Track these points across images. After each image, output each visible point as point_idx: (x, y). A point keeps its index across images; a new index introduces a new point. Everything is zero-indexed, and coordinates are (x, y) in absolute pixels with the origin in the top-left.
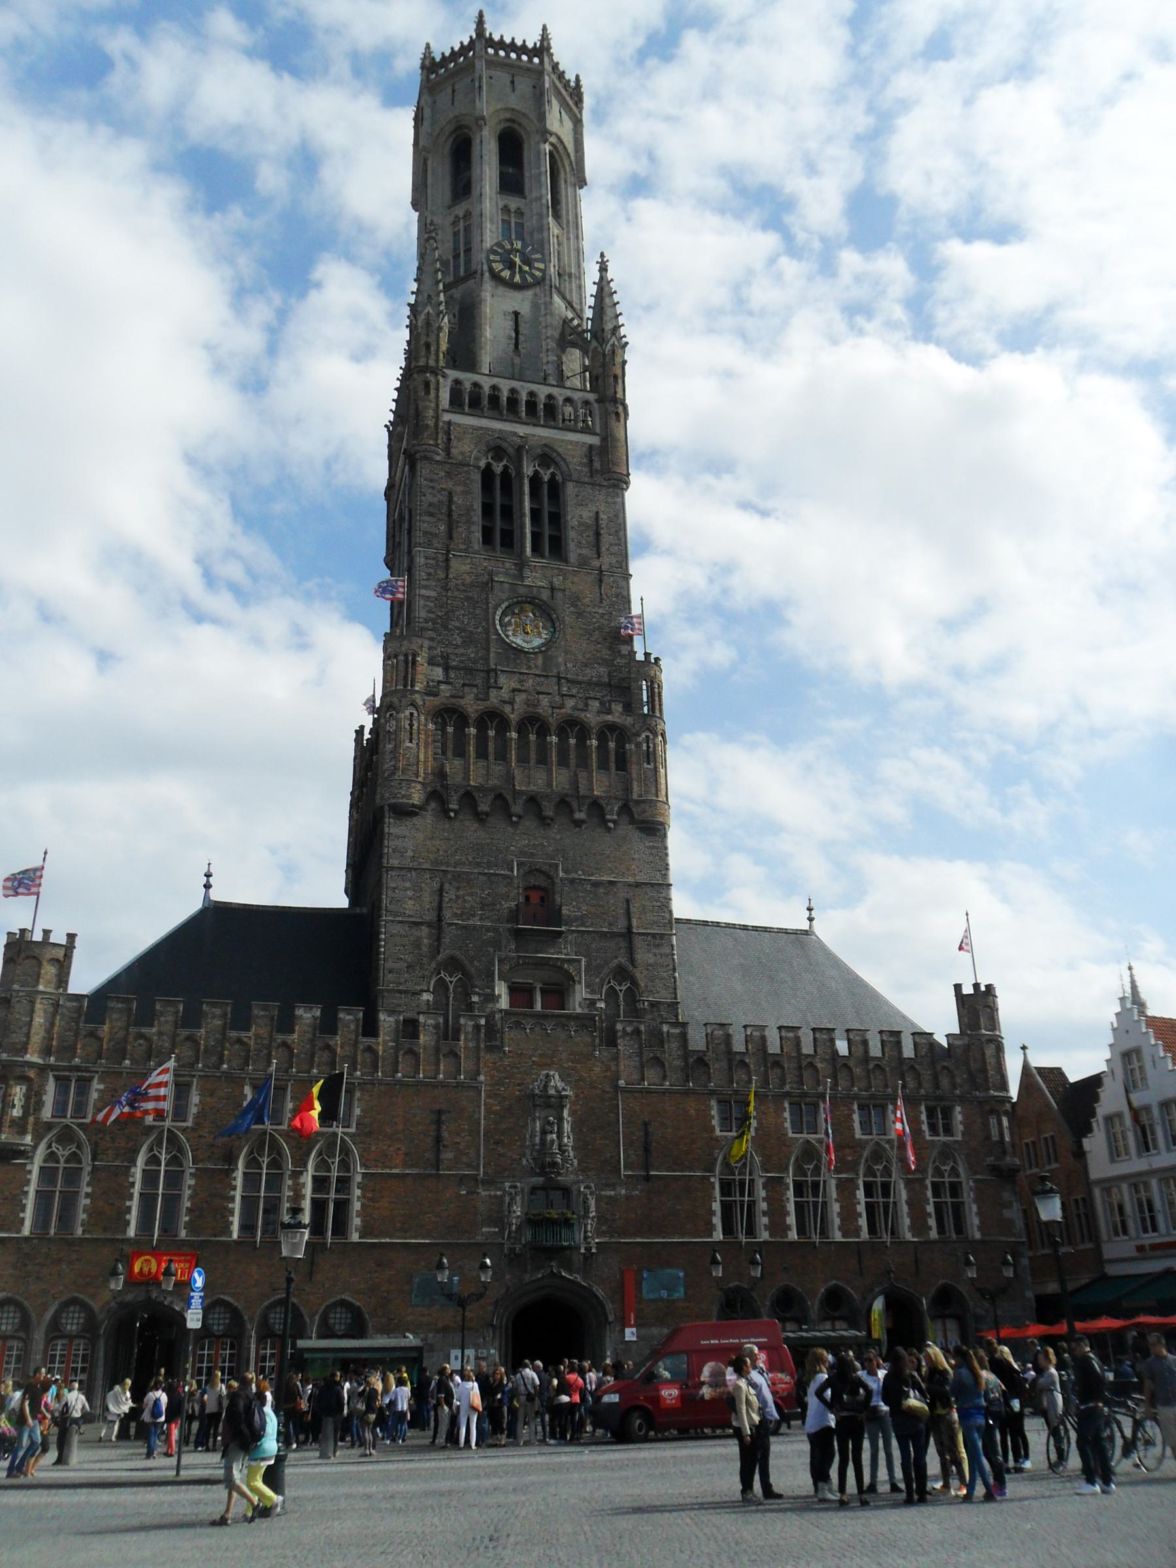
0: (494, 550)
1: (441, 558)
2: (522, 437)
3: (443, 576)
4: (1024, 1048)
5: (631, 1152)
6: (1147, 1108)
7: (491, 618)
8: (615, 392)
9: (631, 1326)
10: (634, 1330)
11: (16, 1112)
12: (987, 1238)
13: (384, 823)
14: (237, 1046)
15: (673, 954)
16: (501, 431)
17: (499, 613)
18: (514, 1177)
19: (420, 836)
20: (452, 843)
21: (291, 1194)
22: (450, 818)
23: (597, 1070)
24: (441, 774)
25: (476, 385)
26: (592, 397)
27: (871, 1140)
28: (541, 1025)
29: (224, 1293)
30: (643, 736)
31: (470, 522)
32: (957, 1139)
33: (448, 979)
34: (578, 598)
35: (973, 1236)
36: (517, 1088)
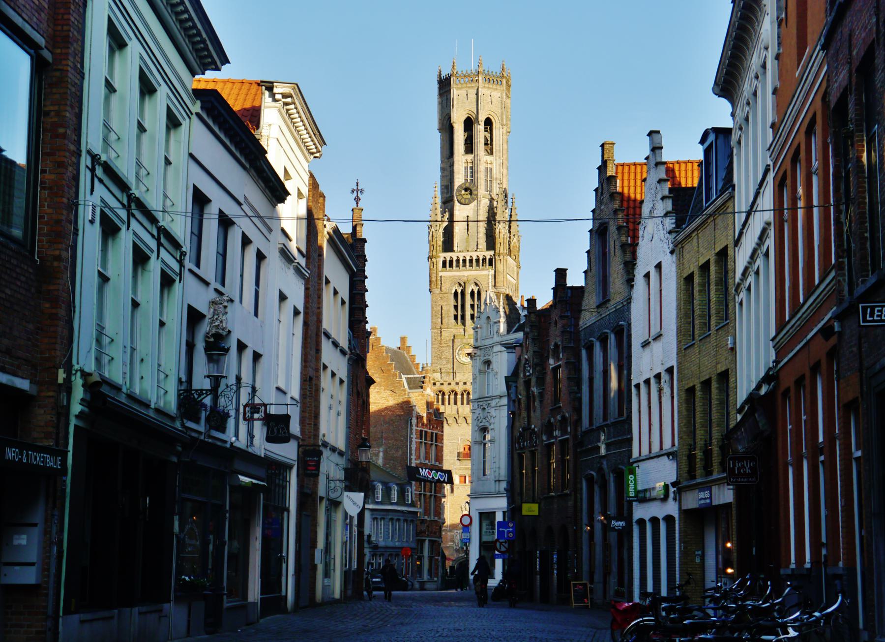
3: (439, 338)
16: (459, 276)
17: (457, 351)
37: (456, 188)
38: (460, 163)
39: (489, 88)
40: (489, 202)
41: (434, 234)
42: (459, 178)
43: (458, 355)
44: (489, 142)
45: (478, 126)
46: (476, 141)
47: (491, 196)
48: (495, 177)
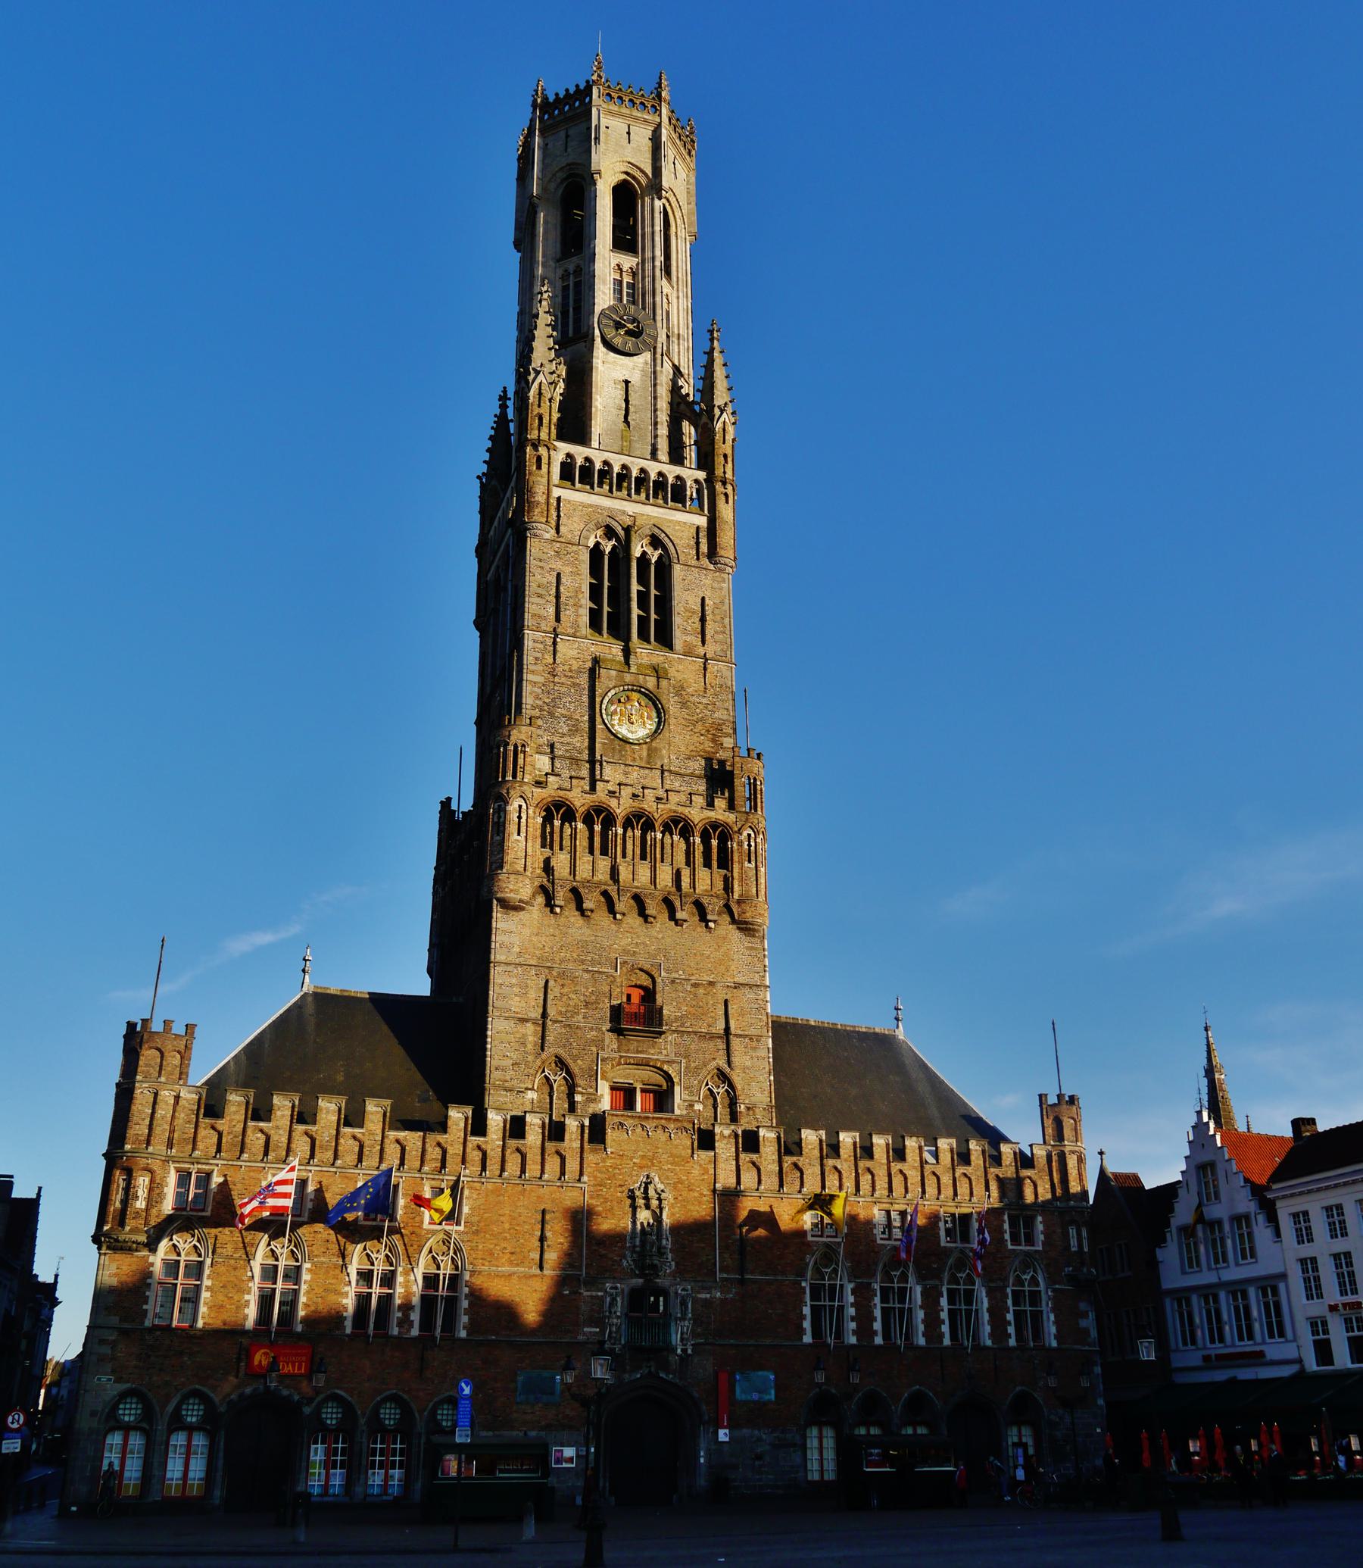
0: (601, 634)
1: (550, 642)
4: (1101, 1153)
5: (726, 1256)
6: (1219, 1222)
7: (598, 706)
8: (725, 473)
9: (725, 1428)
10: (727, 1431)
11: (140, 1204)
12: (1064, 1346)
13: (491, 917)
14: (352, 1141)
15: (769, 1057)
18: (614, 1278)
19: (527, 932)
20: (557, 939)
21: (403, 1291)
22: (557, 914)
23: (696, 1172)
24: (548, 868)
25: (587, 459)
26: (701, 475)
27: (956, 1248)
28: (642, 1126)
29: (338, 1388)
30: (745, 834)
31: (577, 605)
32: (1037, 1248)
33: (552, 1078)
34: (682, 688)
35: (1050, 1344)
36: (620, 1189)
37: (598, 309)
38: (607, 264)
39: (674, 144)
43: (607, 715)
46: (648, 230)
48: (676, 332)
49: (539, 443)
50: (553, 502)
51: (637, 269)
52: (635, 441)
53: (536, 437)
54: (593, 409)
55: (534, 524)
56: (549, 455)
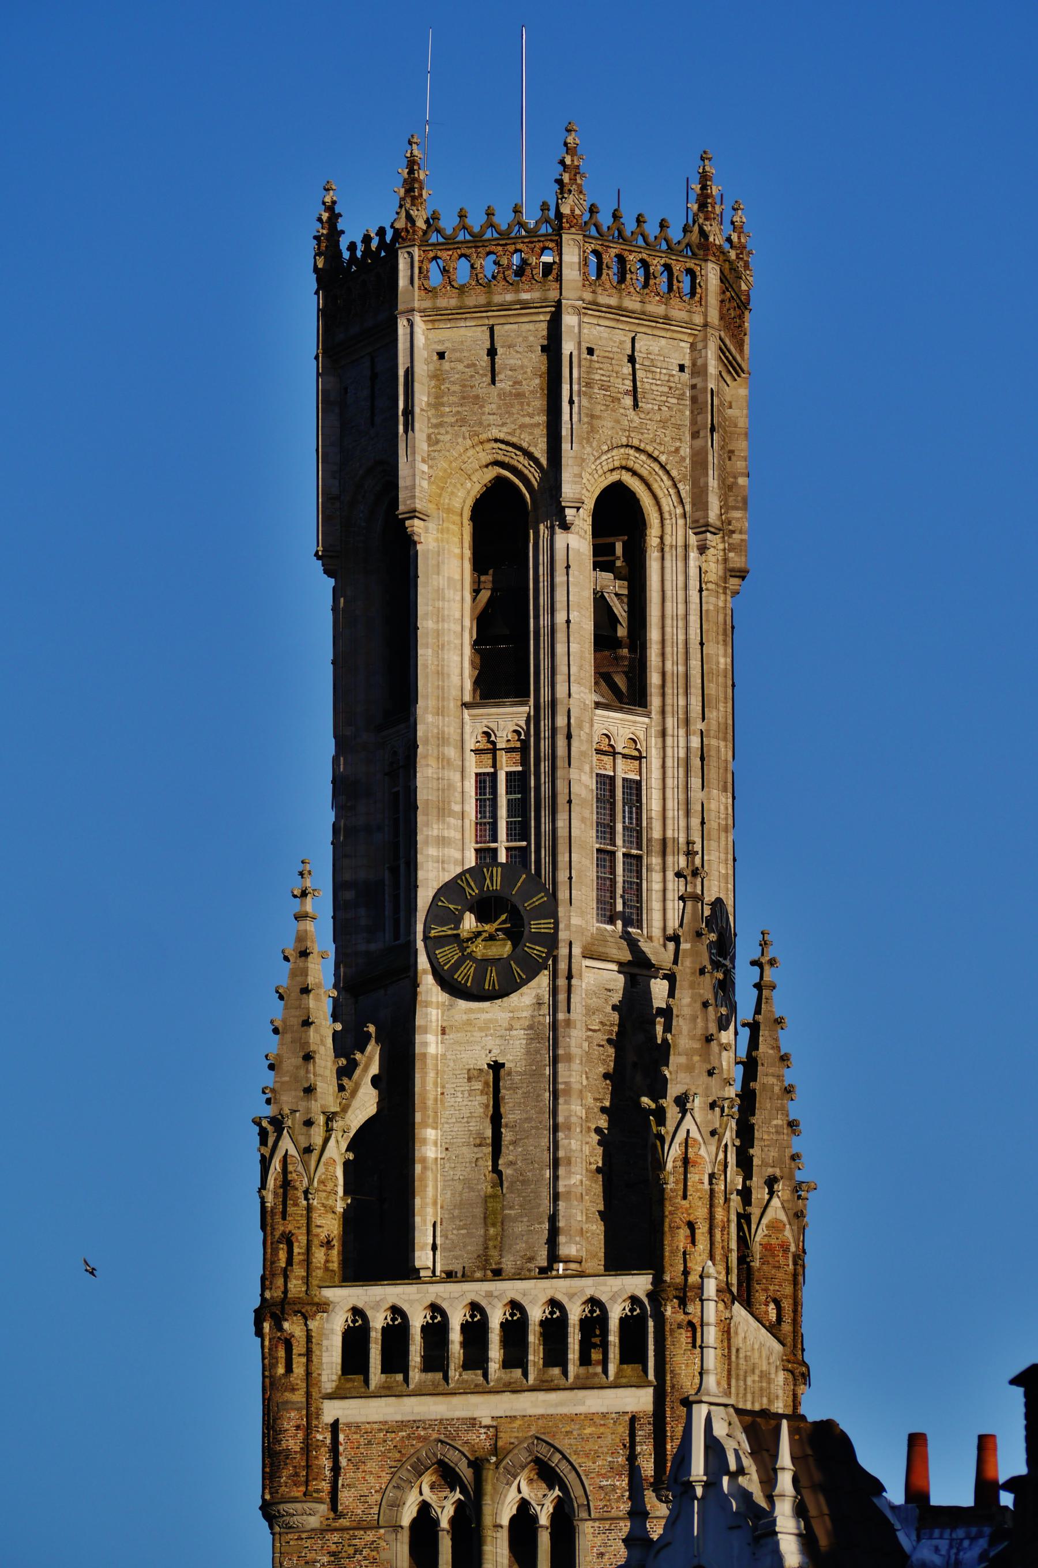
2: (488, 1427)
8: (686, 1273)
25: (396, 1310)
37: (424, 897)
38: (452, 752)
39: (620, 312)
40: (619, 981)
41: (296, 1167)
42: (442, 841)
44: (622, 632)
45: (561, 538)
46: (544, 621)
47: (632, 944)
48: (657, 834)
49: (283, 1312)
50: (323, 1436)
51: (527, 733)
52: (515, 1219)
53: (278, 1294)
54: (418, 1168)
55: (281, 1507)
56: (308, 1331)
